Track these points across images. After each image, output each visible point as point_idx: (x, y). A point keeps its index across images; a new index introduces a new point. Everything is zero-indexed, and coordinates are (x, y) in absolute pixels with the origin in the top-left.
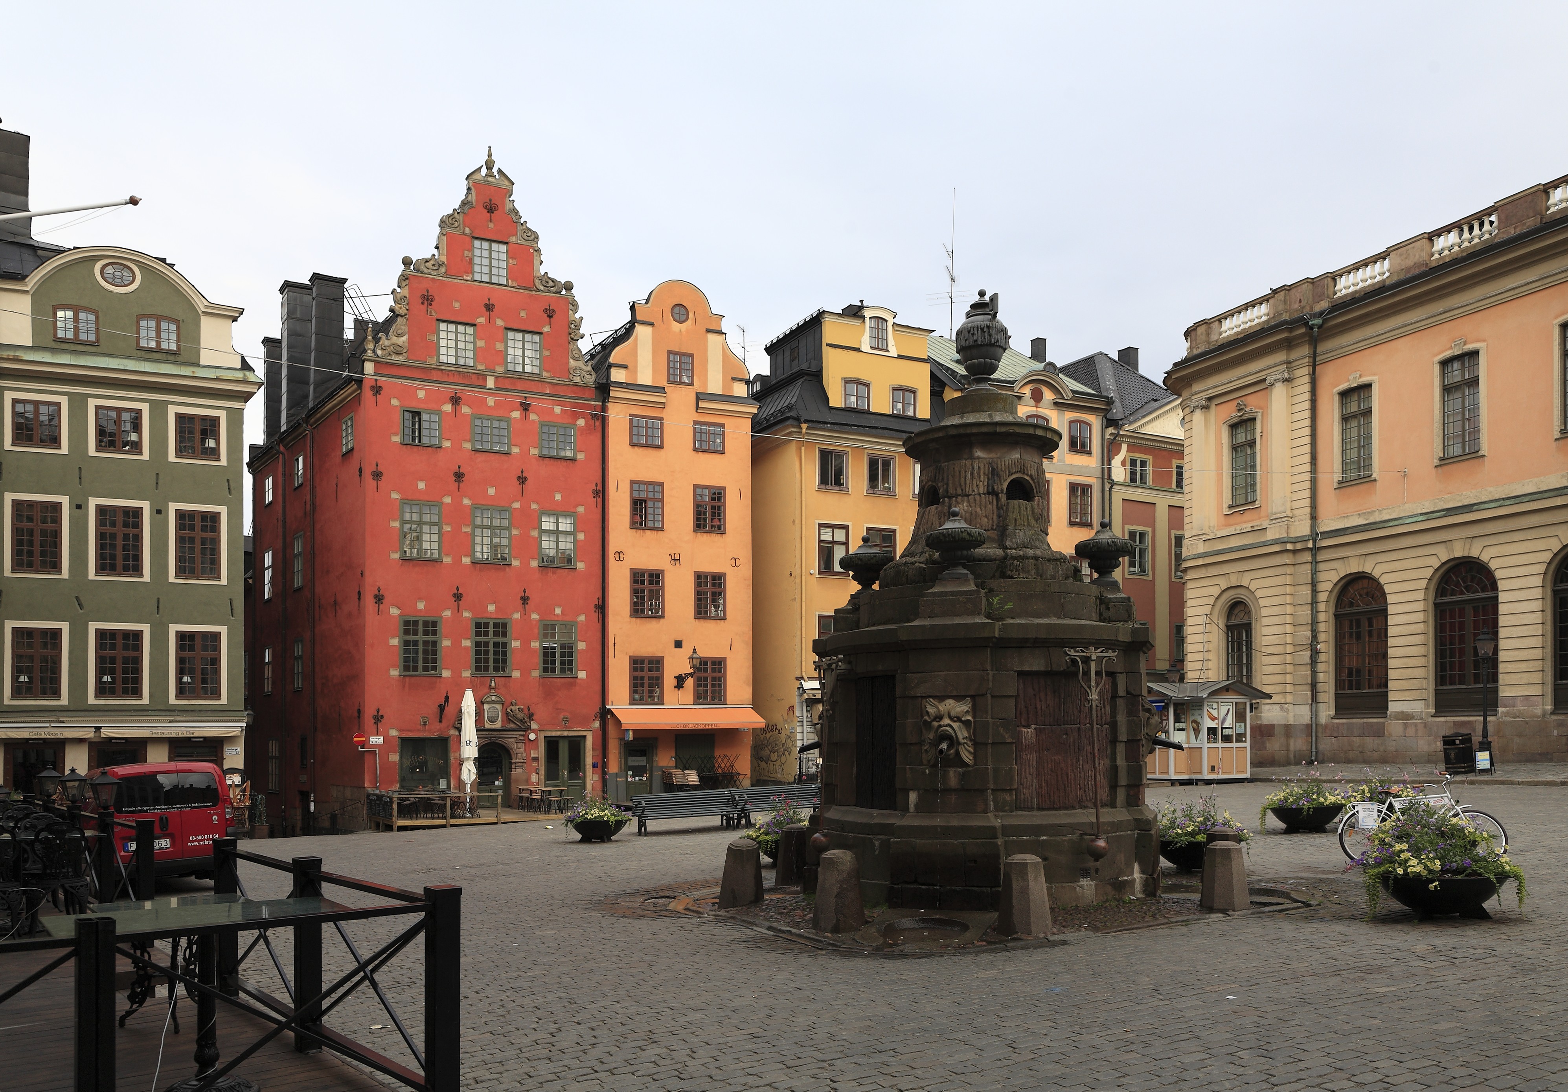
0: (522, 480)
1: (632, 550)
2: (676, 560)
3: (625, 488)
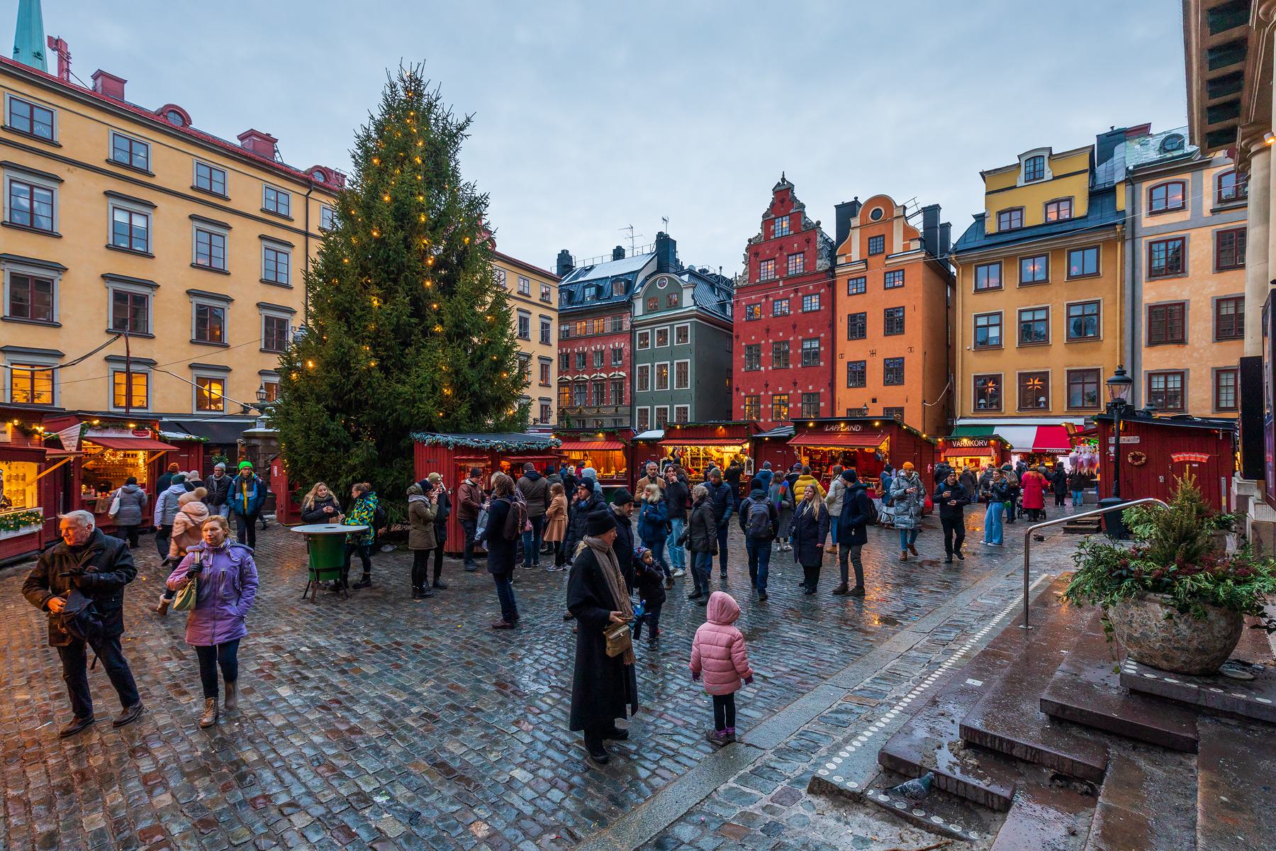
0: (794, 327)
1: (849, 351)
2: (873, 353)
3: (845, 320)
